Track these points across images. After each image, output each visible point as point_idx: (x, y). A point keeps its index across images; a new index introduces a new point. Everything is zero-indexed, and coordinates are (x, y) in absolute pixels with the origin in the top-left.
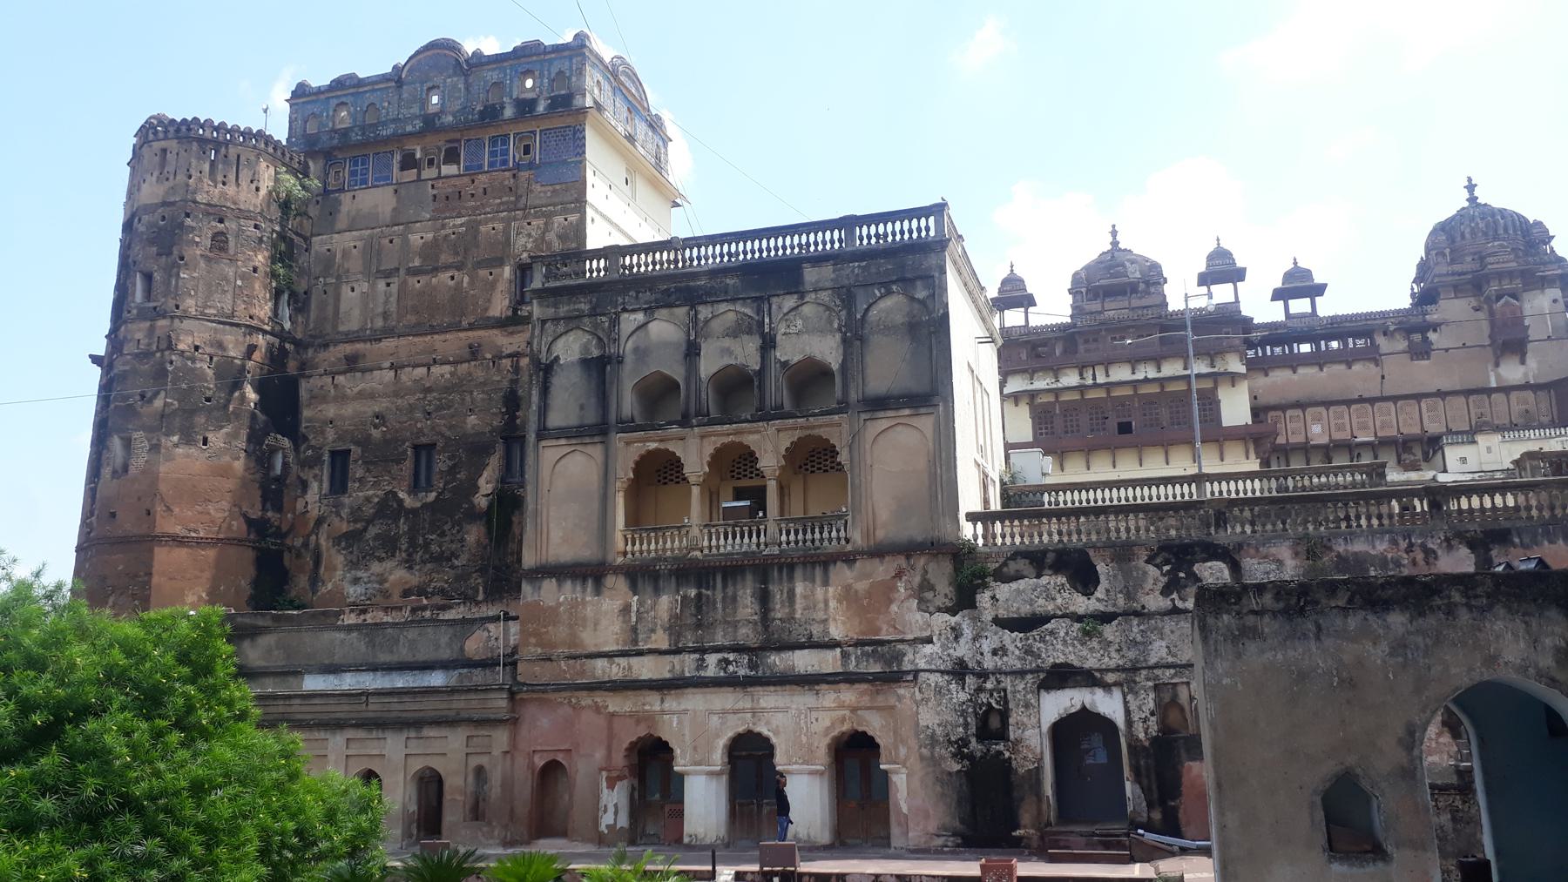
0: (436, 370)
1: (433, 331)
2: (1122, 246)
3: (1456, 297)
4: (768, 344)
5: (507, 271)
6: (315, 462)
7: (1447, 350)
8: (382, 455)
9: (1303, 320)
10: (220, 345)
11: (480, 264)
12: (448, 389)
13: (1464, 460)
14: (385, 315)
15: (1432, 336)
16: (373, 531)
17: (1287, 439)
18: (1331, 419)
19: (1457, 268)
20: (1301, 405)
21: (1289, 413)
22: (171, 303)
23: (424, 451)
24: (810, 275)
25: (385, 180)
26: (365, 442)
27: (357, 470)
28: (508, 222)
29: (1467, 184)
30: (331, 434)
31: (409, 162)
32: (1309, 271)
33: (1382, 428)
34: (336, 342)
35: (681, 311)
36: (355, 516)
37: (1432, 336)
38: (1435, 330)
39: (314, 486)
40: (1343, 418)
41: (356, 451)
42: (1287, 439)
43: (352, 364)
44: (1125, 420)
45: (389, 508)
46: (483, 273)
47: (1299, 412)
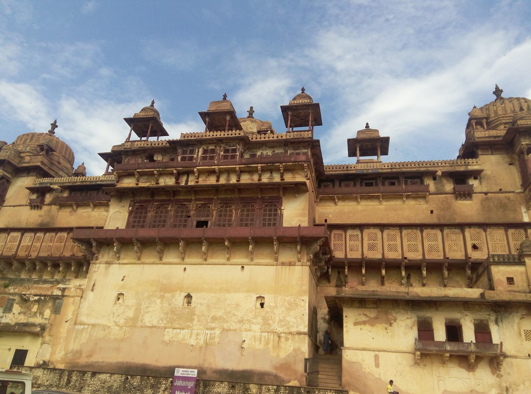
3: (492, 154)
7: (486, 194)
9: (369, 164)
13: (510, 280)
15: (473, 182)
17: (346, 255)
18: (385, 241)
19: (493, 133)
20: (361, 227)
21: (349, 232)
29: (494, 90)
33: (430, 251)
38: (475, 178)
40: (395, 240)
42: (346, 255)
44: (203, 219)
47: (357, 232)
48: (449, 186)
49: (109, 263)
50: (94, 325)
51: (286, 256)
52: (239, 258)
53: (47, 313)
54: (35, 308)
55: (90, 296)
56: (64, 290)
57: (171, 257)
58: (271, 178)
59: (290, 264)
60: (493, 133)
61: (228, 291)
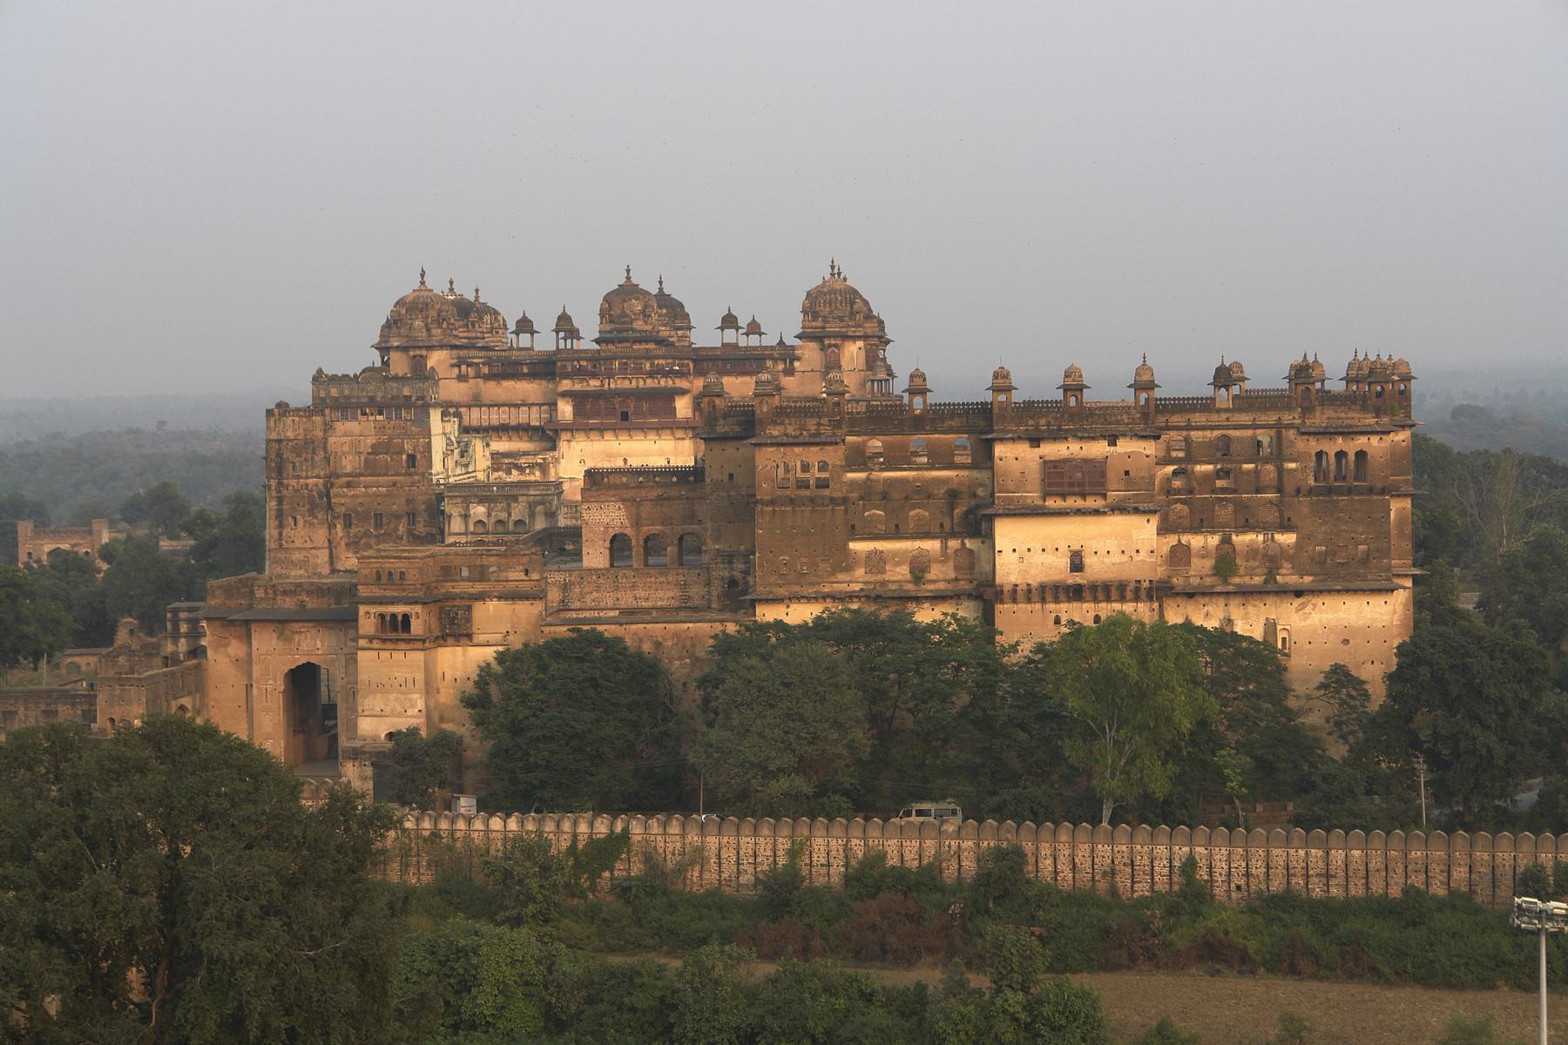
0: (380, 489)
1: (378, 476)
2: (634, 281)
4: (510, 515)
5: (404, 457)
6: (338, 517)
8: (364, 517)
10: (317, 485)
11: (395, 453)
12: (386, 496)
14: (359, 468)
15: (797, 364)
16: (363, 541)
22: (304, 474)
23: (379, 516)
24: (520, 499)
25: (356, 419)
26: (357, 512)
27: (355, 521)
28: (403, 439)
30: (343, 509)
31: (364, 414)
32: (736, 317)
34: (342, 476)
35: (486, 505)
36: (355, 536)
37: (797, 364)
39: (338, 526)
41: (353, 515)
43: (348, 485)
44: (625, 410)
45: (367, 534)
46: (395, 457)
48: (781, 366)
49: (569, 441)
50: (571, 478)
51: (680, 434)
52: (652, 436)
53: (538, 473)
54: (527, 471)
55: (563, 461)
56: (544, 459)
57: (609, 435)
58: (666, 382)
59: (683, 439)
60: (814, 324)
61: (648, 456)
